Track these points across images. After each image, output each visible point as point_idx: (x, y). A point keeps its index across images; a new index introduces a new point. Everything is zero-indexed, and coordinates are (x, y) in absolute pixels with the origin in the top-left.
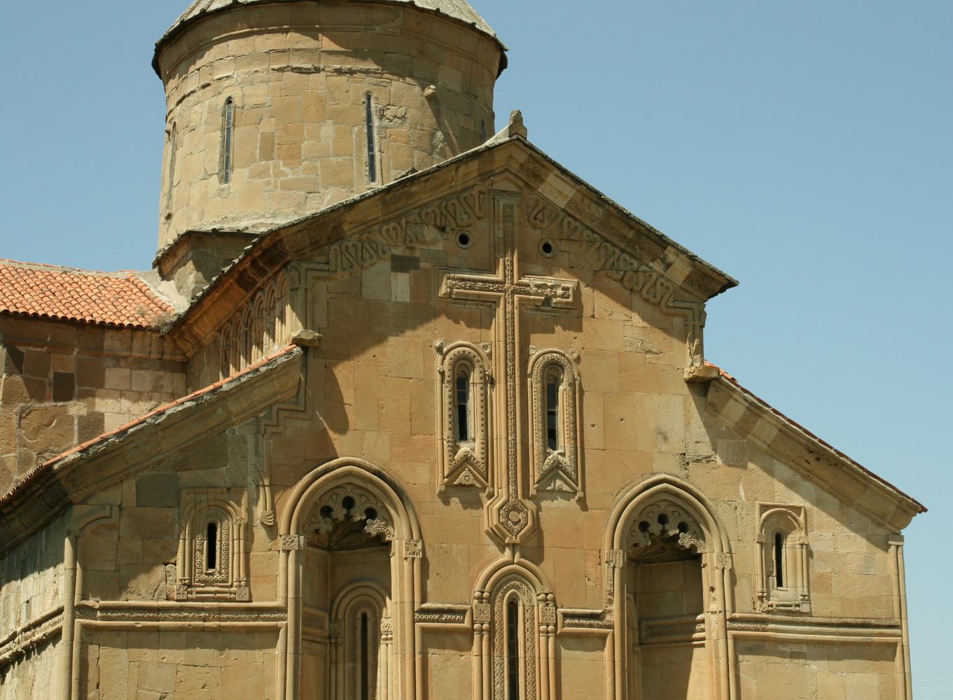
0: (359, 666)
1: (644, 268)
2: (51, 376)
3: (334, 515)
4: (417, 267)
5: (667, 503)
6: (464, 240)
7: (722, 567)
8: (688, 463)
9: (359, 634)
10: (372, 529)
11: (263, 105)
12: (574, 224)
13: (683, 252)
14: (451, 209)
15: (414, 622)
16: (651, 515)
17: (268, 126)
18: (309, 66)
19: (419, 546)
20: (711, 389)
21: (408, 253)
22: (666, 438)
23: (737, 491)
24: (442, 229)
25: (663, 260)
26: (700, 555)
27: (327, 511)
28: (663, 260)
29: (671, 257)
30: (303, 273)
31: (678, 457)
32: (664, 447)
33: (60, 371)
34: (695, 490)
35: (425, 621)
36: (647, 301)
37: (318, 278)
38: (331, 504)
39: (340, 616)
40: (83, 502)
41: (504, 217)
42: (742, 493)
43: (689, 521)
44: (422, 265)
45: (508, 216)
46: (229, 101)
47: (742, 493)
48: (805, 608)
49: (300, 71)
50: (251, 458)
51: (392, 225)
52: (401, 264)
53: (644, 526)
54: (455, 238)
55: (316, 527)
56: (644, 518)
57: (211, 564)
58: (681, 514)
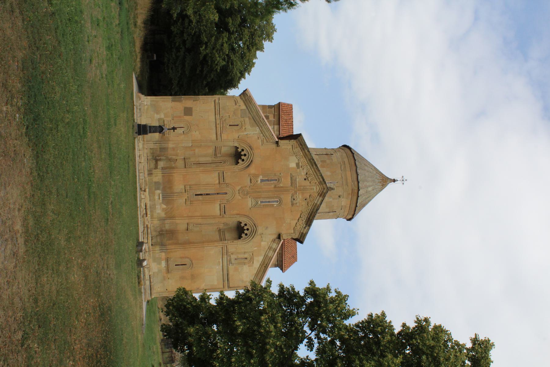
0: (211, 162)
1: (304, 222)
2: (268, 115)
3: (242, 152)
4: (297, 168)
6: (305, 179)
9: (218, 162)
11: (332, 160)
12: (312, 205)
13: (308, 230)
14: (311, 176)
17: (328, 161)
18: (342, 169)
19: (237, 171)
20: (278, 239)
21: (300, 166)
22: (266, 229)
23: (256, 247)
24: (307, 174)
25: (306, 227)
27: (243, 150)
28: (306, 227)
29: (307, 228)
30: (293, 142)
33: (270, 116)
34: (255, 236)
36: (296, 224)
37: (292, 145)
38: (245, 151)
40: (241, 98)
41: (312, 188)
42: (255, 249)
43: (248, 236)
44: (298, 170)
45: (311, 189)
46: (332, 154)
47: (255, 249)
48: (230, 265)
49: (341, 167)
50: (253, 133)
51: (306, 162)
52: (298, 165)
53: (246, 225)
54: (305, 177)
56: (248, 225)
57: (230, 125)
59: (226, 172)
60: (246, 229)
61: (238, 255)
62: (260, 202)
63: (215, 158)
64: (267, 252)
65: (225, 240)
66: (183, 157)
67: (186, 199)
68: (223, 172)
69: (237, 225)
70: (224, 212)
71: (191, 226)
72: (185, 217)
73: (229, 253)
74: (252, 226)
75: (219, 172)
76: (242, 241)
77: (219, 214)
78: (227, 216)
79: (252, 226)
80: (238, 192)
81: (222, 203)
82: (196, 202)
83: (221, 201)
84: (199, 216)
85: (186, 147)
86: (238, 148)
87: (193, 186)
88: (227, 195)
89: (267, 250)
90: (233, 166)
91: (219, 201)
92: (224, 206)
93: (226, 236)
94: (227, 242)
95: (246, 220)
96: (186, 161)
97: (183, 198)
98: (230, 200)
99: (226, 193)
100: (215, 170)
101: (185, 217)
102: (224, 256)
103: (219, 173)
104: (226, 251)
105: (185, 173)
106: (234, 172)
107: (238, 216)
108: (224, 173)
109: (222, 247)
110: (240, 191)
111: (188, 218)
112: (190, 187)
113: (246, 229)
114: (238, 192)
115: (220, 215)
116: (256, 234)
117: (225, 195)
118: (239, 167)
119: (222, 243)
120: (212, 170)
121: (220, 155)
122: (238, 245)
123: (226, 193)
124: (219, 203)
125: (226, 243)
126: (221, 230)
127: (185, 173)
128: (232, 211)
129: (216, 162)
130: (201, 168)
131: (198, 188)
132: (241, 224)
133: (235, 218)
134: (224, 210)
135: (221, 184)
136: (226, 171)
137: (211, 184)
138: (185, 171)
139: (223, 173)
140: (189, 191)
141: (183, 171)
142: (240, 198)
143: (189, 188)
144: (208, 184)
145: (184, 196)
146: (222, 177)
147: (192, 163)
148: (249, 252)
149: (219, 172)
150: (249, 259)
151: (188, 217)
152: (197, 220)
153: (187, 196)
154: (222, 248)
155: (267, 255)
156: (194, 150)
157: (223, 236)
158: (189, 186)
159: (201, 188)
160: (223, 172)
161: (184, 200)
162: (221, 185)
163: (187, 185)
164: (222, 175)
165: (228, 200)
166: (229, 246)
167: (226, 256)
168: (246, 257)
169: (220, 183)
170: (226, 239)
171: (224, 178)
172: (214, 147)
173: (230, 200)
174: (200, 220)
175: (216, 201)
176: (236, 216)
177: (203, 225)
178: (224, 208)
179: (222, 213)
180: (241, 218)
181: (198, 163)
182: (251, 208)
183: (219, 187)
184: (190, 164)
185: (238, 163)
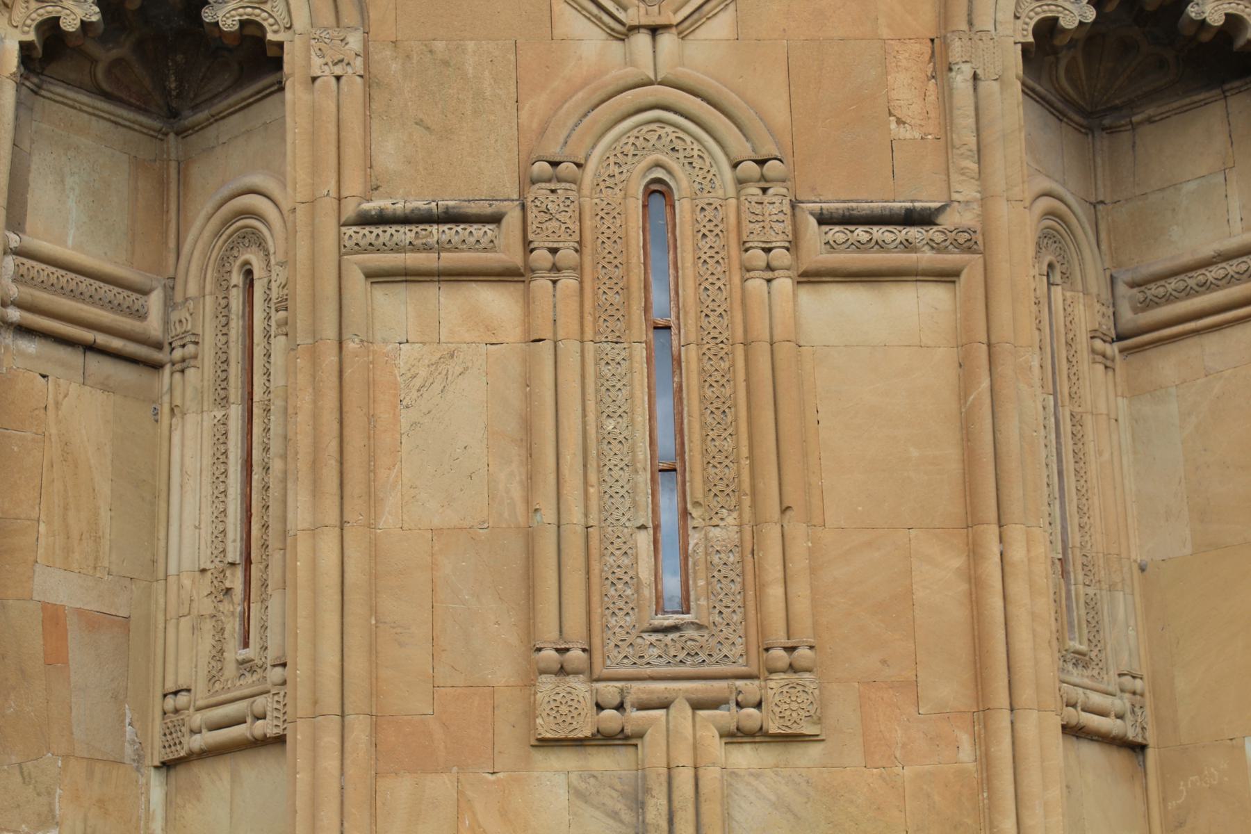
0: (235, 412)
9: (236, 326)
10: (220, 14)
15: (342, 251)
19: (355, 41)
35: (372, 248)
39: (192, 290)
55: (50, 11)
59: (374, 189)
63: (182, 367)
66: (156, 788)
67: (736, 736)
68: (365, 220)
69: (1060, 115)
70: (914, 233)
71: (1097, 699)
72: (985, 761)
75: (356, 281)
77: (936, 295)
78: (967, 191)
80: (643, 39)
81: (793, 246)
82: (775, 592)
83: (758, 258)
84: (974, 552)
85: (166, 820)
86: (50, 28)
87: (548, 631)
88: (682, 184)
90: (294, 92)
91: (756, 284)
92: (824, 220)
93: (1207, 251)
96: (197, 742)
97: (711, 776)
98: (740, 147)
99: (658, 191)
100: (330, 332)
101: (985, 761)
103: (376, 276)
105: (359, 730)
106: (367, 78)
107: (957, 49)
108: (373, 206)
110: (630, 18)
111: (1004, 718)
112: (562, 671)
114: (643, 39)
115: (947, 276)
117: (683, 208)
118: (301, 22)
120: (330, 359)
121: (155, 302)
123: (658, 191)
124: (784, 284)
126: (1129, 318)
127: (359, 730)
129: (236, 353)
130: (300, 514)
131: (574, 580)
132: (1068, 22)
133: (989, 87)
134: (878, 232)
135: (528, 247)
136: (354, 185)
137: (528, 382)
138: (330, 740)
139: (382, 219)
140: (610, 691)
141: (330, 763)
142: (720, 27)
143: (580, 687)
144: (528, 426)
145: (683, 756)
146: (436, 232)
147: (234, 653)
149: (356, 281)
151: (981, 712)
152: (1018, 588)
153: (682, 712)
156: (53, 617)
157: (1206, 287)
158: (547, 685)
159: (575, 515)
160: (365, 220)
161: (745, 757)
162: (541, 257)
163: (531, 713)
164: (405, 234)
165: (750, 168)
169: (511, 255)
171: (451, 218)
172: (30, 347)
173: (740, 147)
174: (1017, 553)
175: (761, 329)
176: (961, 79)
177: (1075, 538)
178: (861, 233)
179: (926, 258)
180: (984, 21)
181: (236, 581)
183: (568, 283)
184: (249, 683)
185: (251, 34)
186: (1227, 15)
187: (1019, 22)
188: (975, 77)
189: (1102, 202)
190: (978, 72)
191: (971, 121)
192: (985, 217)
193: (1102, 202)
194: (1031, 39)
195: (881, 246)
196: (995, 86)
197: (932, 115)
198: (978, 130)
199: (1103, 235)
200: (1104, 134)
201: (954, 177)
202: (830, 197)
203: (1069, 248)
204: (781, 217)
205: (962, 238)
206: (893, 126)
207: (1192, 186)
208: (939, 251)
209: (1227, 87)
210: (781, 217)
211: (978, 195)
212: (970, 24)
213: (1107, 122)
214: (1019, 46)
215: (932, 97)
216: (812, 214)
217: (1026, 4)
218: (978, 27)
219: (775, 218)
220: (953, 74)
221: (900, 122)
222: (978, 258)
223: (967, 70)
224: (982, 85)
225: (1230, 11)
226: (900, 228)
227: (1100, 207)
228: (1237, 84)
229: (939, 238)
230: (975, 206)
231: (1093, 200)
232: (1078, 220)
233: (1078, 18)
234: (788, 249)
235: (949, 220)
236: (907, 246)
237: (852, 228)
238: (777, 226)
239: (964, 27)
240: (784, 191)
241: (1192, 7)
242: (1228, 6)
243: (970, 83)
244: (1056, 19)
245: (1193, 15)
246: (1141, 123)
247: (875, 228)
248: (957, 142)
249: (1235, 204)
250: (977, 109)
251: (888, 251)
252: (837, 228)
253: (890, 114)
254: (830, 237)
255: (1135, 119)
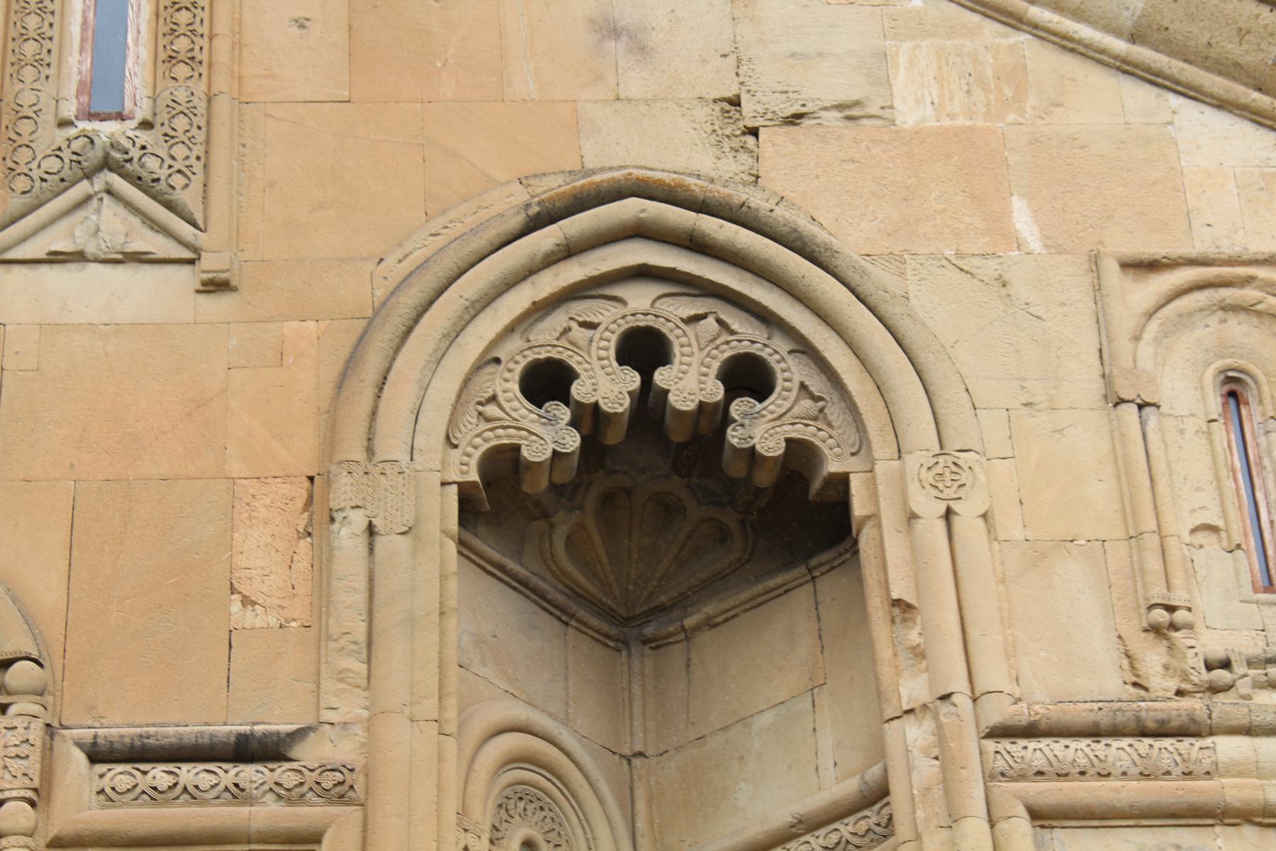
5: (655, 289)
7: (942, 509)
8: (754, 132)
16: (578, 333)
22: (641, 49)
23: (1007, 212)
26: (842, 481)
31: (702, 113)
32: (635, 82)
34: (782, 215)
43: (775, 351)
47: (1022, 219)
58: (735, 326)
60: (633, 379)
61: (1180, 525)
62: (106, 130)
64: (1085, 32)
65: (878, 794)
69: (563, 616)
70: (249, 773)
73: (1161, 684)
74: (574, 272)
76: (882, 447)
78: (350, 706)
79: (574, 272)
89: (1036, 29)
92: (98, 755)
94: (916, 733)
95: (446, 386)
102: (1234, 791)
104: (1119, 751)
107: (344, 489)
109: (1020, 829)
113: (633, 379)
116: (741, 195)
119: (953, 819)
122: (967, 512)
125: (942, 754)
128: (251, 618)
134: (189, 773)
148: (1101, 322)
150: (1240, 330)
154: (1040, 816)
155: (1134, 38)
166: (993, 675)
167: (1229, 747)
168: (1214, 403)
170: (844, 788)
176: (348, 536)
178: (159, 774)
180: (392, 445)
182: (211, 263)
186: (789, 441)
187: (455, 455)
188: (371, 530)
189: (640, 754)
190: (375, 521)
191: (360, 598)
192: (369, 748)
193: (640, 754)
194: (474, 476)
195: (192, 795)
196: (403, 543)
197: (300, 590)
198: (370, 612)
199: (641, 806)
200: (647, 650)
201: (328, 685)
202: (118, 721)
203: (568, 821)
204: (24, 750)
205: (328, 781)
206: (236, 607)
207: (767, 718)
208: (290, 802)
209: (813, 562)
210: (24, 750)
211: (365, 713)
212: (370, 451)
213: (649, 630)
214: (454, 488)
215: (303, 564)
216: (79, 745)
217: (469, 426)
218: (381, 454)
219: (14, 751)
220: (336, 526)
221: (246, 601)
222: (351, 814)
223: (358, 520)
224: (380, 542)
225: (794, 435)
226: (225, 766)
227: (637, 762)
228: (826, 556)
229: (290, 780)
230: (358, 729)
231: (627, 752)
232: (586, 776)
233: (551, 446)
234: (33, 804)
235: (308, 753)
236: (238, 794)
237: (143, 767)
238: (15, 765)
239: (360, 455)
240: (37, 709)
241: (734, 430)
242: (791, 427)
243: (362, 541)
244: (516, 449)
245: (735, 441)
246: (697, 628)
247: (185, 767)
248: (335, 631)
249: (826, 741)
250: (371, 580)
251: (205, 802)
252: (120, 768)
253: (233, 590)
254: (106, 783)
255: (689, 622)
